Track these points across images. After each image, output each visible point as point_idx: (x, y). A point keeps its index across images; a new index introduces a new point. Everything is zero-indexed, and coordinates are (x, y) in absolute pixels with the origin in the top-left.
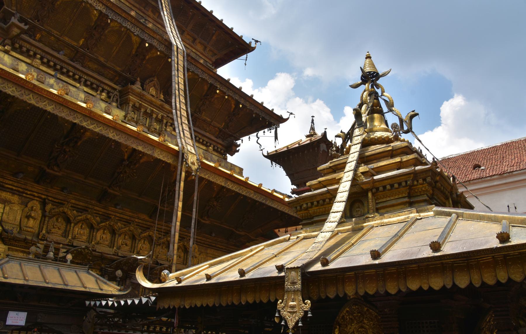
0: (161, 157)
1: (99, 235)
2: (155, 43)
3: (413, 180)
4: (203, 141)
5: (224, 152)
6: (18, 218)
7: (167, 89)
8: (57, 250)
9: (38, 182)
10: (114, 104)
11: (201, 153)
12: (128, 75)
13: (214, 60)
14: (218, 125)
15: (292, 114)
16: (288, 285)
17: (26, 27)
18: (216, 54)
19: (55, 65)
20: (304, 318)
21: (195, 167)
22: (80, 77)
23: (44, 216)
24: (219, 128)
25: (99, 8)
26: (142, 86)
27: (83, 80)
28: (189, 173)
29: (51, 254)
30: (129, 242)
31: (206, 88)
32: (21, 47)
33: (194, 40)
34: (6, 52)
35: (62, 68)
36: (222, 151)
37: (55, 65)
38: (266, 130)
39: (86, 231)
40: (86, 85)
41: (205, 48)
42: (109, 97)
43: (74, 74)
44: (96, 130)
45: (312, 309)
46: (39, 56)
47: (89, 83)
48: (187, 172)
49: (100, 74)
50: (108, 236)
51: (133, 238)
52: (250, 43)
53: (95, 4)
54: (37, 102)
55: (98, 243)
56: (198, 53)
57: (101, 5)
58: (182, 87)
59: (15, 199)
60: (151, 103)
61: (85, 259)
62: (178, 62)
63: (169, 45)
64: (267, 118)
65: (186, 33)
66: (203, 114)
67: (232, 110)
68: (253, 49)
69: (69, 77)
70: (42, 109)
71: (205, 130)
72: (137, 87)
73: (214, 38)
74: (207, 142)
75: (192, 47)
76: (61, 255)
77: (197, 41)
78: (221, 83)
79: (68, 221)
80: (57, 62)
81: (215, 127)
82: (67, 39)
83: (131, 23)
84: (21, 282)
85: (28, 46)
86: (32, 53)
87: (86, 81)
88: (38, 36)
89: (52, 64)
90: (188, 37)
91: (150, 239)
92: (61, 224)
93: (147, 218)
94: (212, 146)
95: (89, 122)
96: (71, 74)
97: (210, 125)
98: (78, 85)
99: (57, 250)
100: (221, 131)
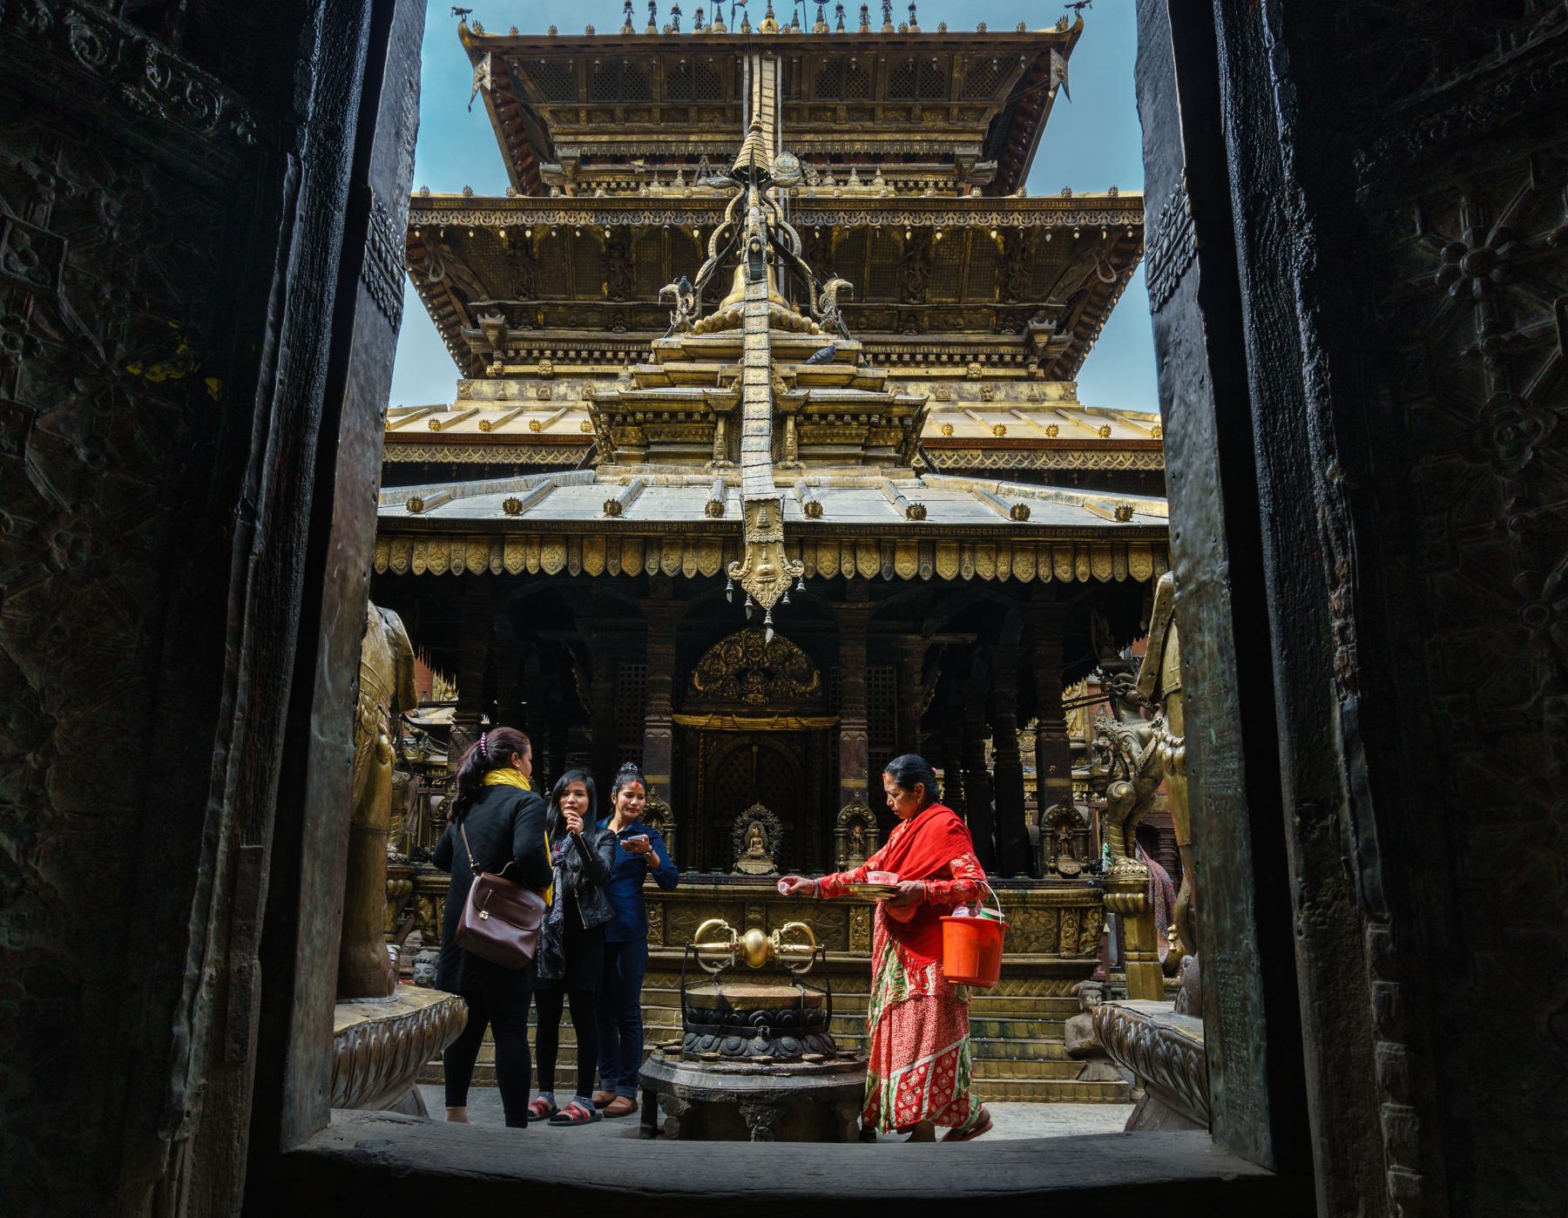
4: (951, 357)
5: (1025, 358)
13: (984, 125)
18: (985, 110)
19: (578, 353)
22: (628, 353)
32: (517, 352)
33: (908, 111)
35: (591, 353)
36: (1019, 358)
37: (578, 353)
41: (947, 112)
43: (615, 354)
46: (548, 353)
54: (457, 456)
56: (934, 136)
57: (583, 214)
65: (879, 112)
66: (928, 296)
69: (610, 362)
71: (960, 330)
73: (956, 75)
74: (963, 356)
75: (908, 131)
77: (917, 111)
78: (911, 212)
80: (578, 346)
81: (976, 309)
82: (581, 299)
83: (650, 211)
85: (526, 345)
86: (536, 353)
88: (540, 317)
89: (572, 354)
90: (891, 115)
94: (982, 358)
96: (609, 355)
97: (960, 310)
100: (998, 311)
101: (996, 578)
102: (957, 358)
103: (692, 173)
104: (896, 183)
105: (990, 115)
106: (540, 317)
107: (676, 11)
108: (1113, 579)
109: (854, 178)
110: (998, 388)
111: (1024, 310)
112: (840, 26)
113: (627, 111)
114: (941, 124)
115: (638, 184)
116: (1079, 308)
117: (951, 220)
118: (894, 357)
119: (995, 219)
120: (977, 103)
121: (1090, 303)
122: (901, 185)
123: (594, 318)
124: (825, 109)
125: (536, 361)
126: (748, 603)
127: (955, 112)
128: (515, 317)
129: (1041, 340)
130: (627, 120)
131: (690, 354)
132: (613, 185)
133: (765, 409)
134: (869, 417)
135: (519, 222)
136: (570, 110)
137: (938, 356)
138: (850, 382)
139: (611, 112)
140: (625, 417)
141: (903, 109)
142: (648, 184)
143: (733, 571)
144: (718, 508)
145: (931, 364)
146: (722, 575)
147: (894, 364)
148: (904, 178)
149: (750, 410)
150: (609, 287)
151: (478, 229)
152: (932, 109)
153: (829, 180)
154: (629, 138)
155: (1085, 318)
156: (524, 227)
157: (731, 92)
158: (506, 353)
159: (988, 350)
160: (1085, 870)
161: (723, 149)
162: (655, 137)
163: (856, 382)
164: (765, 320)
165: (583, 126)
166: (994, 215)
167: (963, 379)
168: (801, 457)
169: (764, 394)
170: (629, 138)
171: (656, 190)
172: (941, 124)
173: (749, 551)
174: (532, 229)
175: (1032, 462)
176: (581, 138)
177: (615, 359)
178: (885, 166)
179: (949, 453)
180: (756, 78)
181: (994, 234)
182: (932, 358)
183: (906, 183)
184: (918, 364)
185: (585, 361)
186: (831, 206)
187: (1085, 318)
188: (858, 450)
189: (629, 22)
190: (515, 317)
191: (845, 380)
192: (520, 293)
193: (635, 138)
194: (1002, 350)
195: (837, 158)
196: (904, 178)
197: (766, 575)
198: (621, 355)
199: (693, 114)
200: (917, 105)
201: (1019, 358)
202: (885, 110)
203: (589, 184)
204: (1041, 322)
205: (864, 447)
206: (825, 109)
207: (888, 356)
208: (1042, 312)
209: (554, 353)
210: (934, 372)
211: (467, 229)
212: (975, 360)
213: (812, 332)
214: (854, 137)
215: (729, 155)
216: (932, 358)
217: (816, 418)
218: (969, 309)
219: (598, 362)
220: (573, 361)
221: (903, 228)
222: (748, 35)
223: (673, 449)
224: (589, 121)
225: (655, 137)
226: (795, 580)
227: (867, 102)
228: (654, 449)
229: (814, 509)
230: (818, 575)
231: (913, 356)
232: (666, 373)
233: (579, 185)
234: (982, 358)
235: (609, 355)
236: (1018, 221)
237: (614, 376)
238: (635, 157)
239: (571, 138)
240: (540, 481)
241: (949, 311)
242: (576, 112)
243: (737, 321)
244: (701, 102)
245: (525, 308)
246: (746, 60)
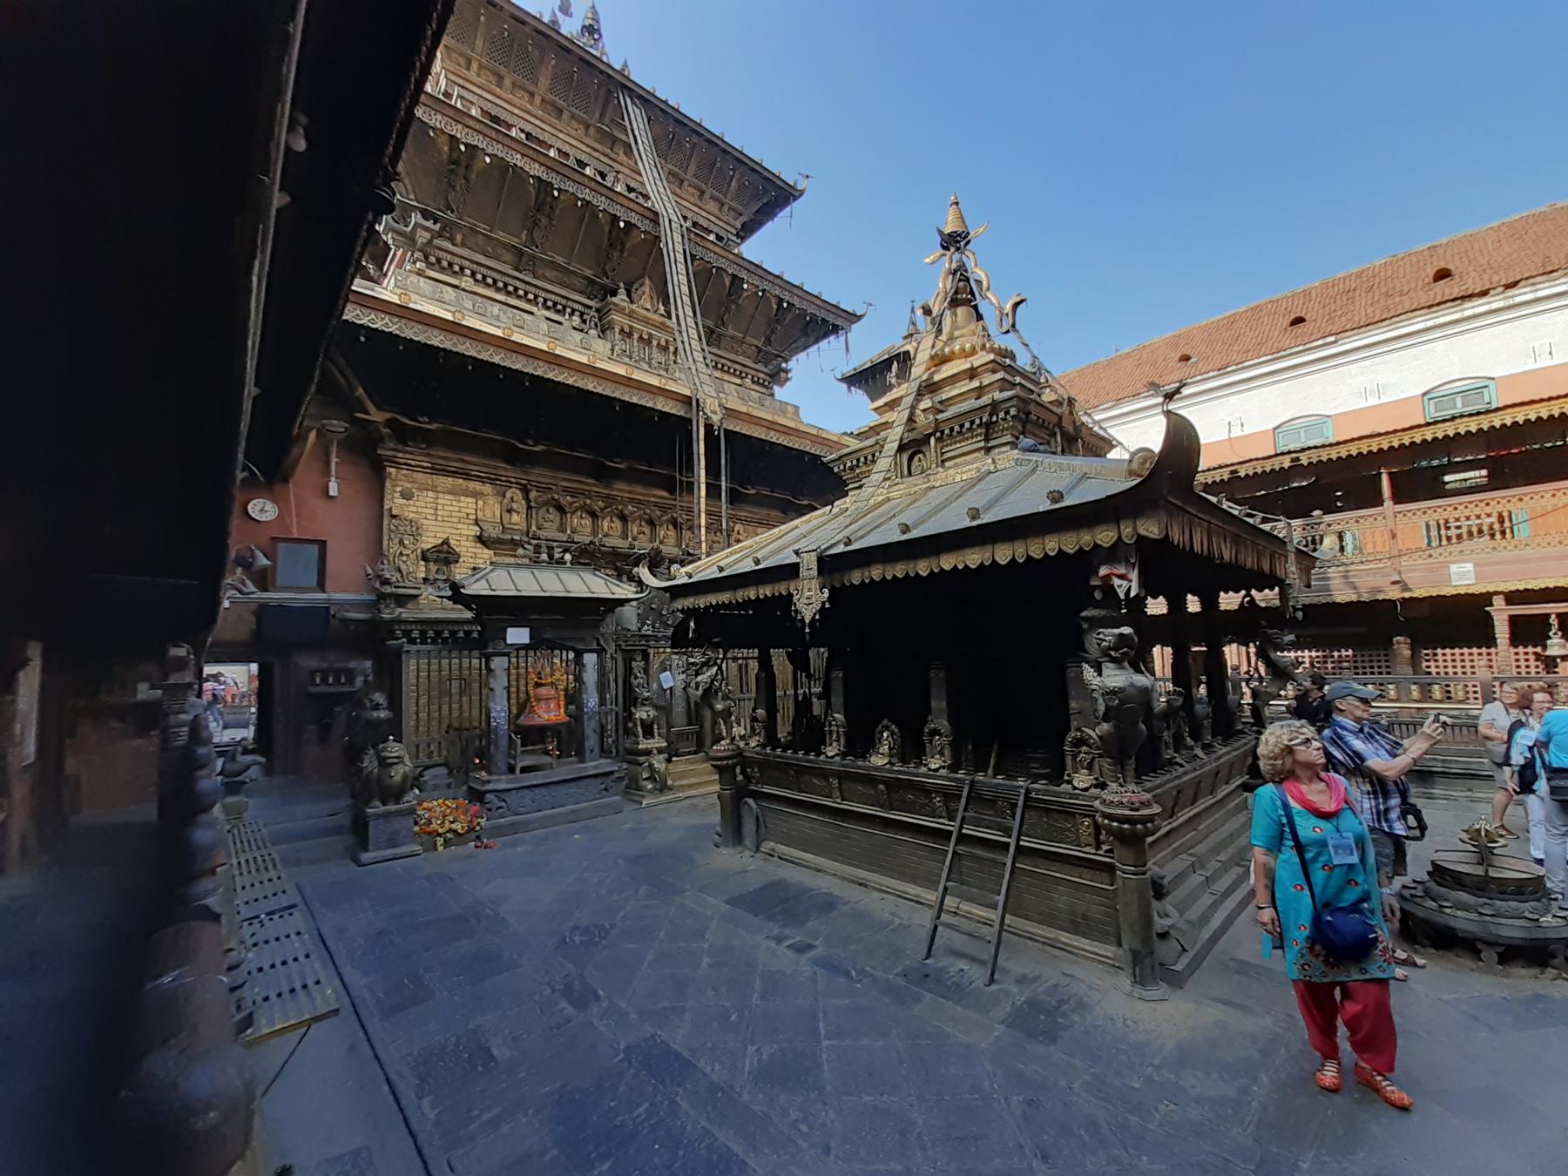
0: (666, 409)
1: (606, 524)
2: (634, 219)
3: (991, 416)
6: (498, 513)
7: (663, 295)
8: (551, 549)
9: (509, 463)
10: (592, 332)
12: (605, 281)
16: (803, 572)
17: (437, 227)
20: (822, 610)
21: (715, 419)
22: (536, 297)
23: (529, 507)
26: (629, 296)
27: (540, 300)
28: (709, 427)
29: (544, 557)
30: (647, 529)
31: (727, 281)
32: (439, 260)
34: (420, 273)
38: (832, 338)
39: (588, 521)
40: (548, 308)
42: (584, 322)
43: (526, 293)
45: (830, 599)
46: (468, 272)
47: (550, 304)
48: (706, 426)
49: (563, 285)
50: (617, 524)
51: (651, 523)
55: (606, 535)
58: (685, 289)
59: (488, 488)
60: (646, 321)
61: (588, 557)
62: (674, 246)
63: (654, 217)
64: (831, 319)
68: (802, 192)
69: (519, 297)
72: (621, 298)
76: (557, 556)
77: (707, 196)
79: (561, 510)
82: (501, 235)
84: (514, 593)
85: (449, 257)
86: (457, 268)
88: (459, 238)
91: (674, 522)
92: (553, 514)
93: (665, 494)
96: (521, 293)
98: (534, 309)
99: (551, 549)
100: (760, 350)
105: (743, 219)
114: (717, 212)
120: (740, 208)
123: (508, 257)
157: (597, 115)
172: (717, 212)
185: (498, 290)
190: (447, 231)
193: (516, 111)
200: (709, 191)
239: (461, 82)
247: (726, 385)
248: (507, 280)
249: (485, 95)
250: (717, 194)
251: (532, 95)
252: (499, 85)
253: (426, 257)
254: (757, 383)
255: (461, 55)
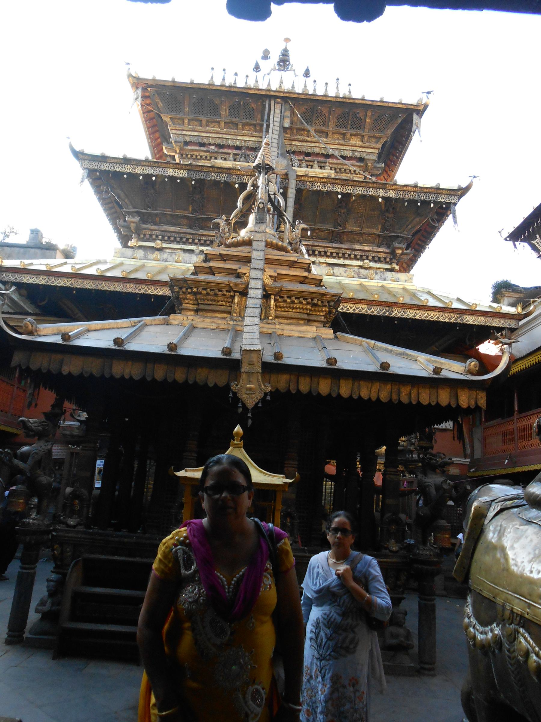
4: (355, 256)
5: (391, 259)
11: (343, 273)
14: (374, 231)
15: (475, 177)
19: (175, 238)
22: (199, 240)
24: (374, 234)
25: (181, 176)
35: (181, 239)
36: (388, 260)
43: (193, 240)
44: (160, 294)
52: (422, 99)
53: (176, 174)
56: (355, 148)
65: (330, 134)
67: (383, 206)
68: (426, 106)
69: (190, 244)
70: (113, 291)
71: (360, 243)
73: (368, 120)
74: (361, 256)
77: (348, 136)
78: (342, 185)
81: (369, 234)
82: (178, 213)
83: (215, 172)
86: (154, 237)
87: (205, 241)
89: (172, 239)
90: (336, 136)
94: (370, 258)
95: (153, 289)
96: (190, 241)
100: (379, 236)
101: (370, 399)
102: (358, 257)
103: (238, 154)
104: (335, 169)
105: (382, 141)
106: (158, 219)
107: (236, 74)
108: (430, 403)
109: (316, 165)
110: (376, 274)
111: (392, 237)
112: (315, 91)
113: (208, 121)
115: (211, 158)
116: (417, 237)
117: (360, 191)
118: (328, 254)
119: (381, 193)
121: (422, 235)
122: (338, 170)
123: (185, 222)
124: (304, 130)
125: (154, 241)
126: (240, 405)
127: (366, 138)
128: (145, 219)
129: (399, 252)
130: (207, 126)
131: (223, 258)
132: (199, 157)
133: (259, 293)
134: (312, 300)
135: (150, 173)
136: (179, 119)
137: (350, 255)
138: (304, 280)
139: (200, 121)
140: (187, 289)
141: (341, 134)
142: (216, 158)
143: (233, 387)
144: (227, 351)
145: (345, 258)
146: (227, 387)
147: (328, 257)
148: (340, 166)
149: (251, 293)
150: (193, 207)
151: (129, 174)
152: (356, 135)
153: (304, 165)
154: (208, 135)
155: (419, 242)
156: (152, 175)
157: (259, 117)
158: (139, 235)
159: (373, 254)
160: (401, 549)
161: (254, 145)
162: (221, 136)
163: (307, 280)
164: (263, 244)
165: (186, 127)
166: (381, 190)
167: (361, 267)
168: (276, 317)
169: (259, 284)
170: (208, 135)
171: (220, 163)
172: (359, 143)
173: (244, 376)
174: (156, 176)
175: (390, 313)
176: (184, 133)
177: (193, 243)
178: (330, 160)
179: (352, 305)
180: (272, 112)
181: (380, 200)
182: (347, 256)
183: (340, 169)
184: (340, 258)
185: (178, 242)
186: (304, 178)
187: (419, 242)
188: (305, 316)
189: (212, 78)
190: (145, 219)
191: (302, 279)
192: (148, 207)
193: (210, 135)
194: (380, 255)
195: (308, 154)
196: (340, 166)
197: (251, 390)
198: (196, 241)
199: (240, 126)
201: (388, 260)
202: (333, 133)
203: (187, 155)
204: (400, 243)
205: (308, 314)
206: (304, 130)
207: (326, 253)
208: (400, 239)
209: (163, 237)
210: (347, 262)
211: (123, 173)
212: (367, 258)
213: (287, 251)
214: (317, 145)
215: (256, 148)
216: (347, 256)
217: (285, 298)
218: (365, 234)
219: (184, 243)
220: (171, 242)
221: (337, 193)
222: (269, 90)
223: (211, 308)
224: (189, 125)
225: (221, 136)
226: (266, 394)
227: (325, 129)
228: (201, 307)
229: (278, 356)
230: (277, 390)
231: (338, 254)
232: (210, 268)
233: (182, 155)
234: (370, 258)
235: (190, 241)
236: (392, 194)
237: (192, 251)
238: (210, 144)
240: (140, 322)
241: (357, 234)
242: (183, 120)
243: (248, 243)
244: (244, 121)
245: (150, 214)
246: (267, 102)
247: (337, 270)
248: (182, 235)
249: (193, 133)
250: (353, 132)
251: (219, 122)
252: (201, 126)
253: (139, 235)
254: (379, 261)
255: (179, 119)
